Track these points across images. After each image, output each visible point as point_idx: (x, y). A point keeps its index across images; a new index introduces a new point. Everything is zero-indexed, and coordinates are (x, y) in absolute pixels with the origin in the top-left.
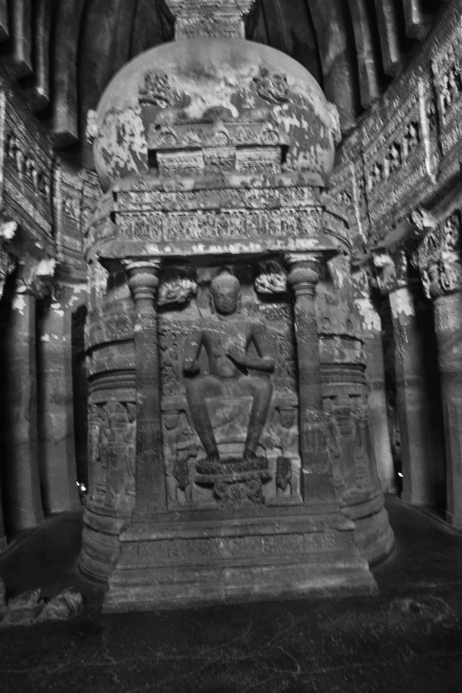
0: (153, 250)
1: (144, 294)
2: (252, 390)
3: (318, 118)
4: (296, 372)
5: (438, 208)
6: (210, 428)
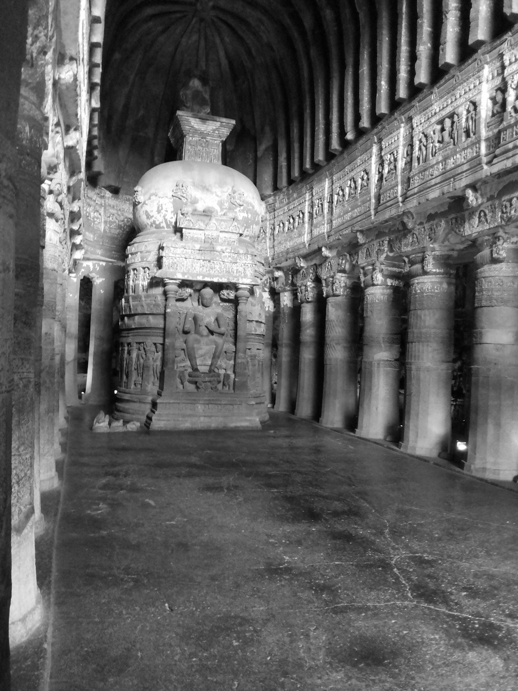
0: (180, 276)
3: (256, 211)
4: (236, 337)
5: (308, 258)
6: (195, 358)
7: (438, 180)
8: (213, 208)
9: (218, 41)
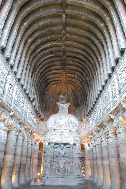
0: (54, 142)
1: (53, 147)
2: (65, 159)
3: (76, 124)
4: (70, 158)
6: (59, 164)
7: (106, 112)
8: (63, 124)
9: (69, 86)
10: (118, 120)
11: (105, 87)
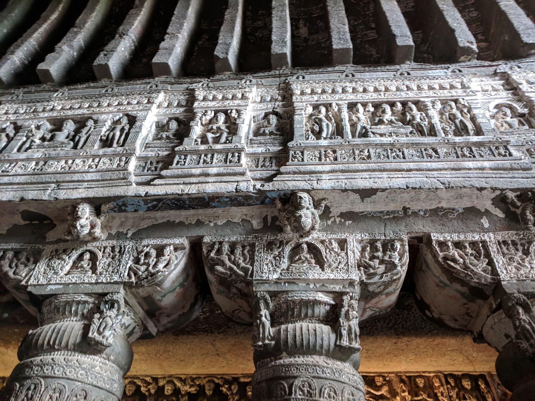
10: (130, 263)
11: (104, 82)
